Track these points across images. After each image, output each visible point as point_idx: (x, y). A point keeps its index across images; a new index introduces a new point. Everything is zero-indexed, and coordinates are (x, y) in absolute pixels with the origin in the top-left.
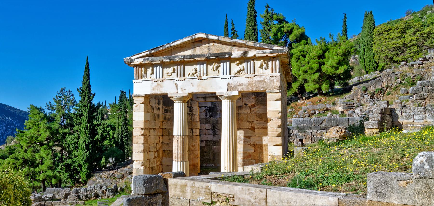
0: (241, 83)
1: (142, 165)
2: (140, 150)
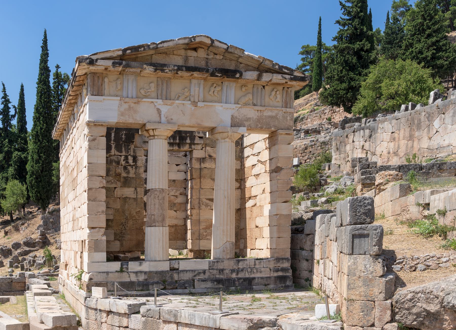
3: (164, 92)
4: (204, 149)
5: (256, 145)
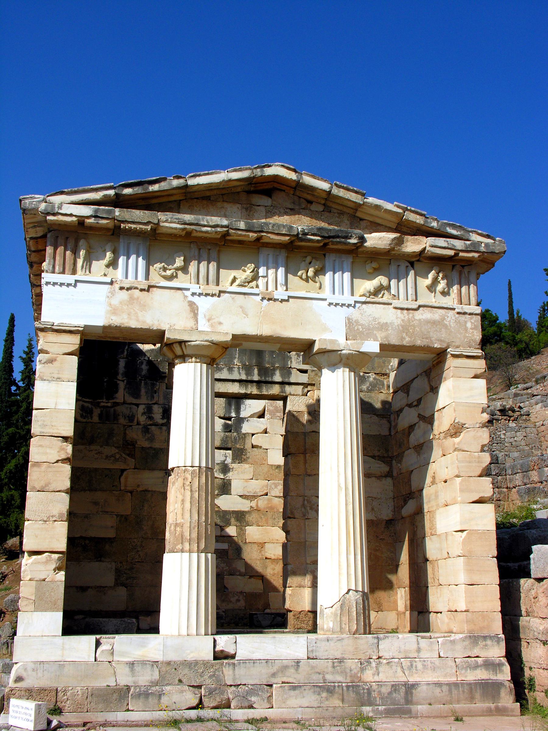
0: (383, 321)
1: (59, 569)
5: (414, 385)
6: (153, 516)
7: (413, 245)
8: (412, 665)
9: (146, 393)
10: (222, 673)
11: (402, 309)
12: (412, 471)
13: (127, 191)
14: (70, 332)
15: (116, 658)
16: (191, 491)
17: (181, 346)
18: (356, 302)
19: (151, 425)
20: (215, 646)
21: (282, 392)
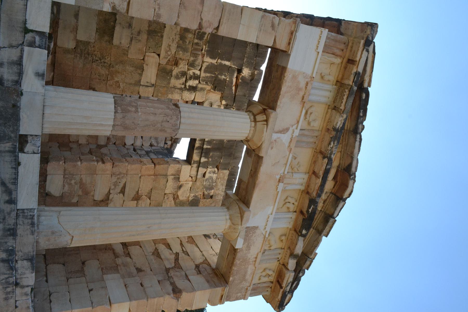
1: (114, 8)
2: (162, 11)
3: (305, 139)
4: (190, 179)
6: (125, 73)
7: (292, 264)
8: (10, 284)
9: (207, 77)
10: (7, 143)
11: (256, 258)
12: (141, 247)
13: (364, 95)
14: (289, 44)
15: (26, 49)
16: (162, 122)
17: (264, 121)
18: (266, 231)
19: (186, 77)
20: (31, 135)
21: (194, 162)
